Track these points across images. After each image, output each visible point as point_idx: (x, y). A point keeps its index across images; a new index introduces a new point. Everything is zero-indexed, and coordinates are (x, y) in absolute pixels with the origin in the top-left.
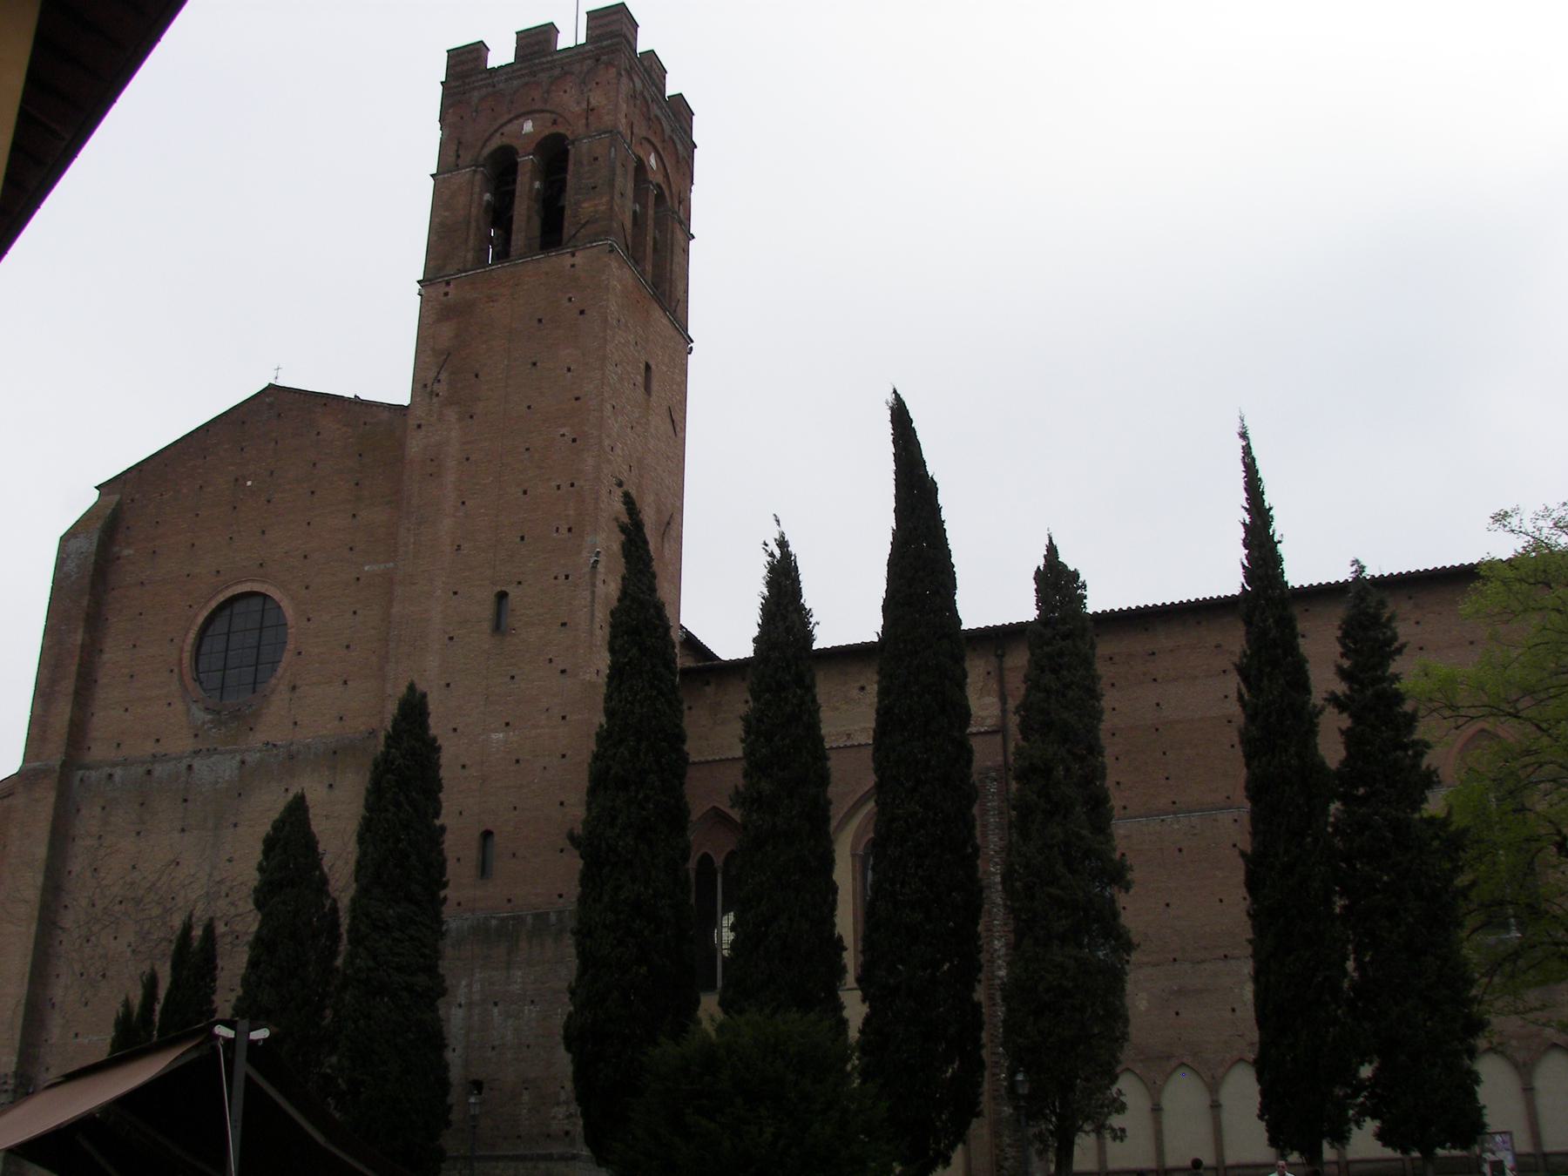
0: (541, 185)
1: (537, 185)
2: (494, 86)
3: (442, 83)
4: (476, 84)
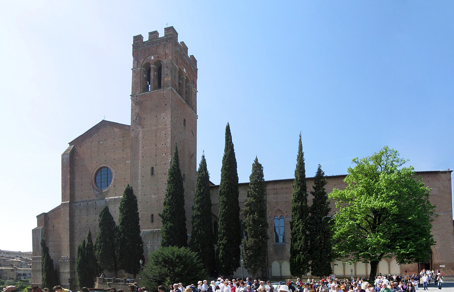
0: (157, 73)
1: (156, 73)
2: (144, 47)
3: (132, 45)
4: (140, 46)
